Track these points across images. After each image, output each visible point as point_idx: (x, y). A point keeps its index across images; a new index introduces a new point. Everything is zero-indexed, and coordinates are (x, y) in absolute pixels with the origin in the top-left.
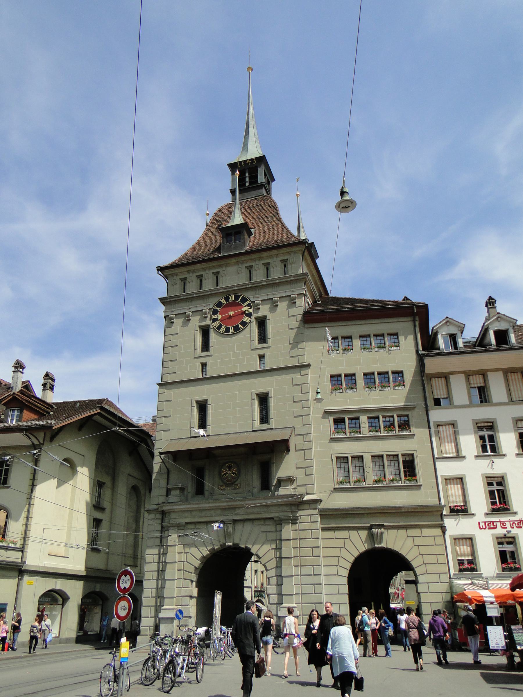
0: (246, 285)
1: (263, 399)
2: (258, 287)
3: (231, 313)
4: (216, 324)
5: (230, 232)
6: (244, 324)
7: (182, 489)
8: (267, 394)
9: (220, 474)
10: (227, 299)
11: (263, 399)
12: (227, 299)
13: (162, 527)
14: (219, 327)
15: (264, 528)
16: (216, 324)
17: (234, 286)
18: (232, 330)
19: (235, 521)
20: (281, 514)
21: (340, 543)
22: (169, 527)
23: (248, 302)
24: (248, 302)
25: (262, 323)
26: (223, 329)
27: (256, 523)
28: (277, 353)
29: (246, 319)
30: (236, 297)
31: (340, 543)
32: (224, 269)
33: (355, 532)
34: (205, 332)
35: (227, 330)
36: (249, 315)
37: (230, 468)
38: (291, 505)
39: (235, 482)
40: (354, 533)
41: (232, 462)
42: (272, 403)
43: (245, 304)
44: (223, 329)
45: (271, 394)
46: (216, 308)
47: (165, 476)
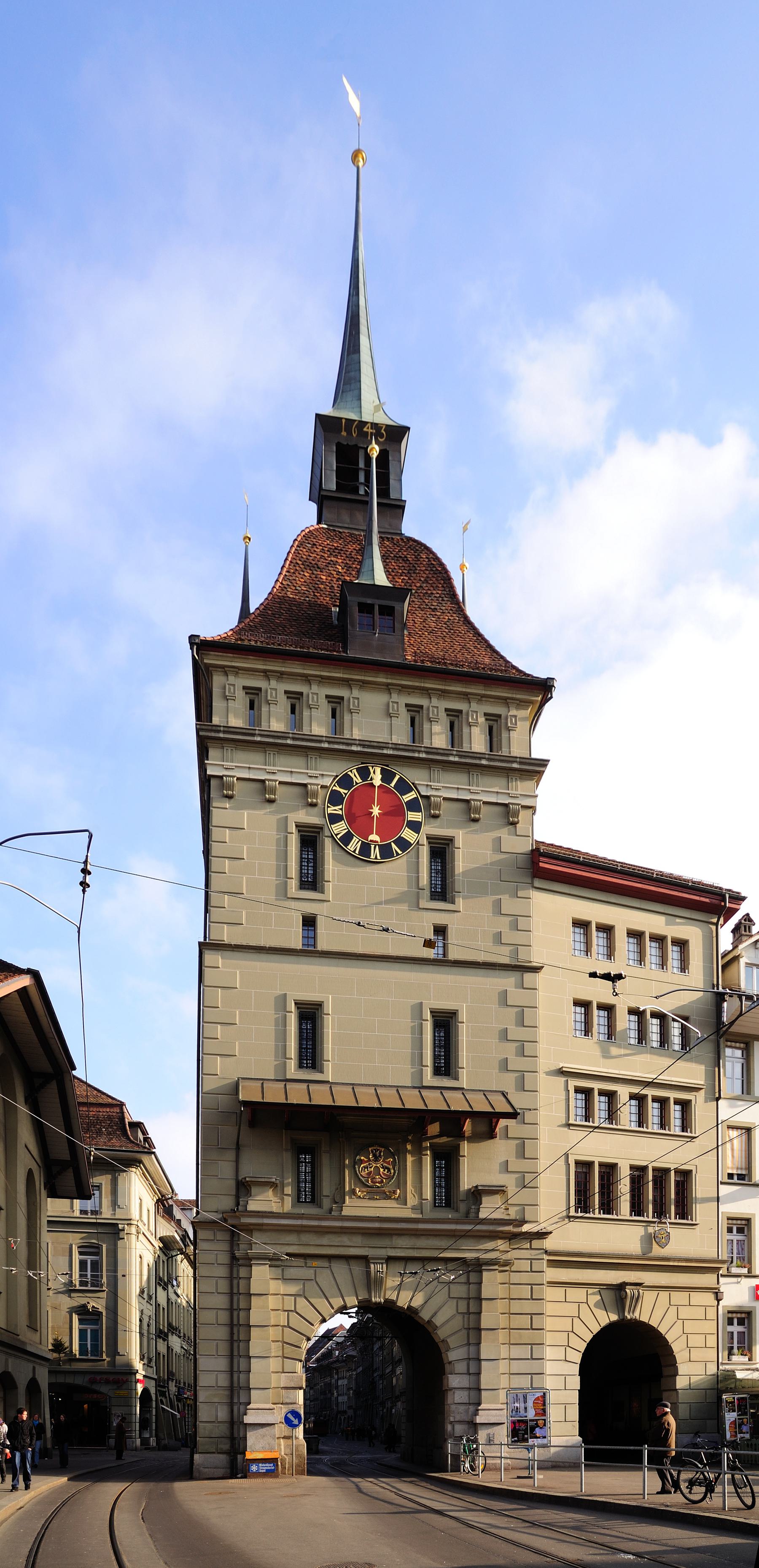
2: (435, 762)
3: (376, 811)
4: (340, 828)
6: (404, 844)
10: (364, 773)
12: (364, 773)
14: (347, 839)
16: (340, 828)
18: (375, 853)
23: (411, 796)
24: (411, 796)
25: (441, 851)
26: (355, 845)
29: (408, 834)
30: (387, 776)
32: (356, 693)
34: (310, 840)
35: (365, 849)
36: (415, 827)
43: (407, 798)
44: (355, 845)
46: (338, 788)
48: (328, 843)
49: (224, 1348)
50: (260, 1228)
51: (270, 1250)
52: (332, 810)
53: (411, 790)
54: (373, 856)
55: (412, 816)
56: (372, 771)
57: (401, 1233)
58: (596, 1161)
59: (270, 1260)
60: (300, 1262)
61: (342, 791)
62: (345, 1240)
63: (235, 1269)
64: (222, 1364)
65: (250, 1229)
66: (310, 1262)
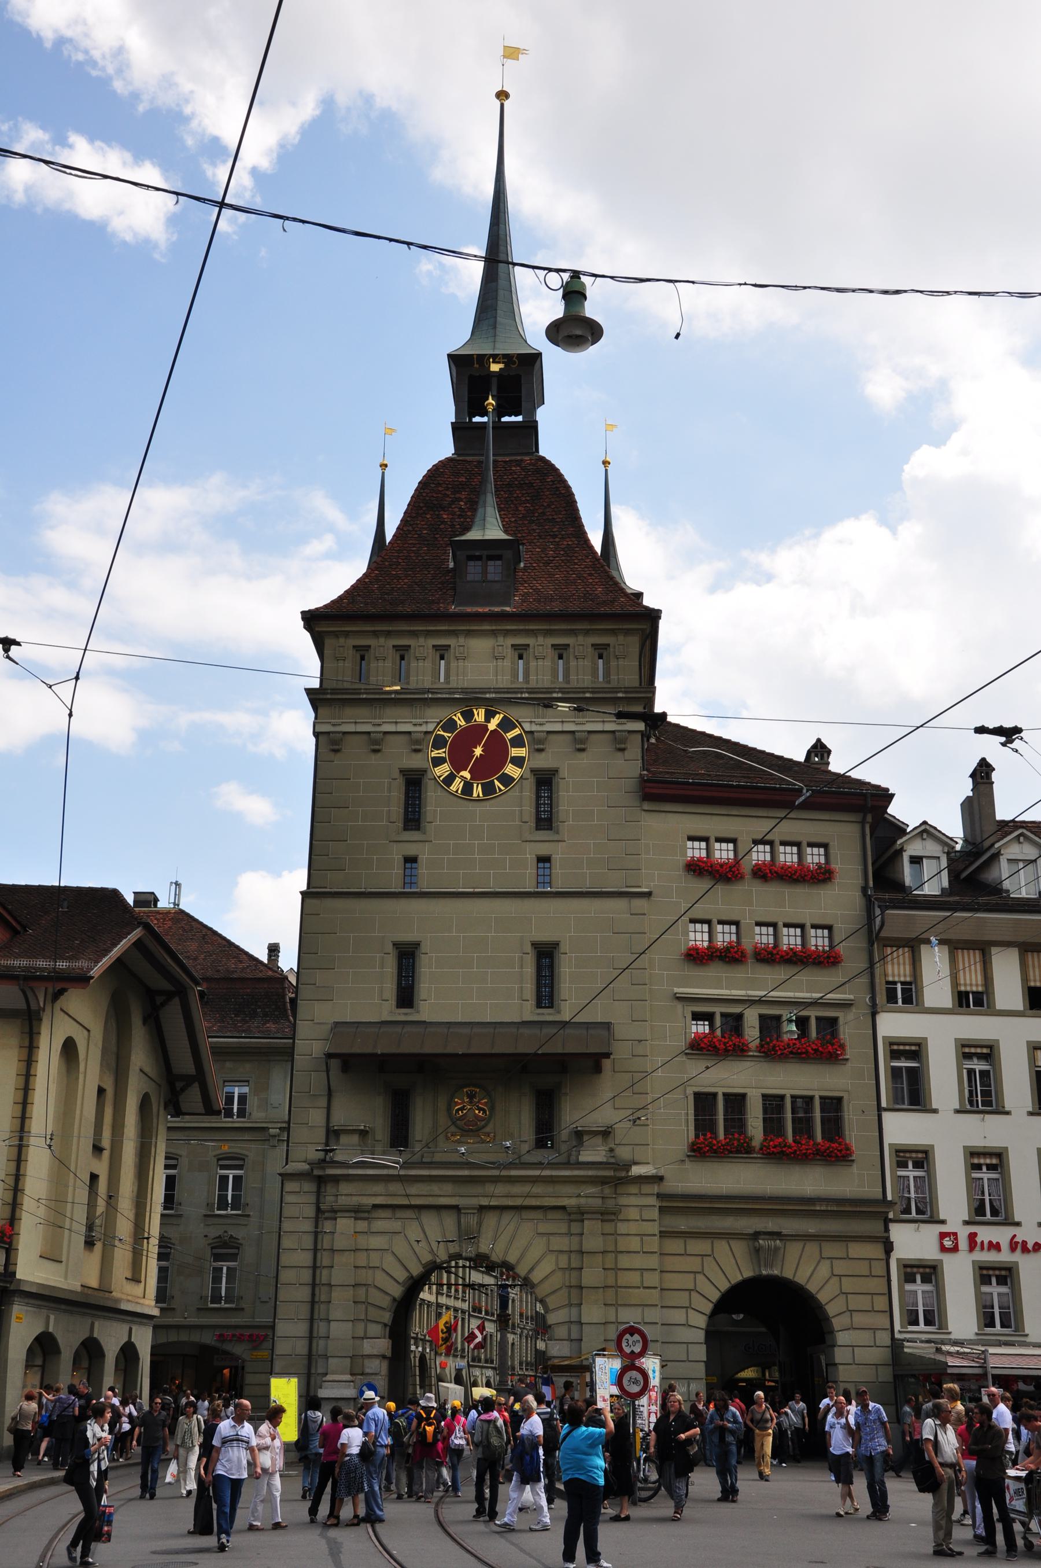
0: (516, 693)
1: (546, 955)
4: (443, 770)
5: (477, 554)
6: (507, 780)
7: (363, 1133)
8: (556, 945)
9: (449, 1109)
10: (468, 716)
11: (546, 955)
12: (468, 716)
13: (318, 1210)
14: (449, 780)
15: (543, 1228)
16: (443, 770)
17: (488, 690)
19: (482, 1208)
20: (583, 1201)
21: (694, 1264)
22: (336, 1212)
23: (516, 732)
24: (516, 732)
27: (526, 1214)
28: (575, 854)
29: (511, 770)
31: (694, 1264)
32: (462, 640)
33: (724, 1243)
36: (518, 762)
37: (471, 1096)
38: (603, 1181)
39: (483, 1127)
40: (722, 1247)
41: (475, 1086)
42: (566, 968)
43: (510, 735)
45: (564, 947)
46: (442, 733)
47: (324, 1102)
48: (431, 784)
49: (304, 1311)
50: (348, 1178)
51: (355, 1200)
52: (435, 754)
53: (515, 727)
54: (475, 795)
55: (515, 752)
56: (476, 712)
57: (495, 1180)
58: (720, 1091)
59: (355, 1212)
60: (387, 1213)
61: (446, 734)
62: (435, 1188)
63: (320, 1223)
64: (301, 1329)
65: (336, 1179)
66: (400, 1214)
